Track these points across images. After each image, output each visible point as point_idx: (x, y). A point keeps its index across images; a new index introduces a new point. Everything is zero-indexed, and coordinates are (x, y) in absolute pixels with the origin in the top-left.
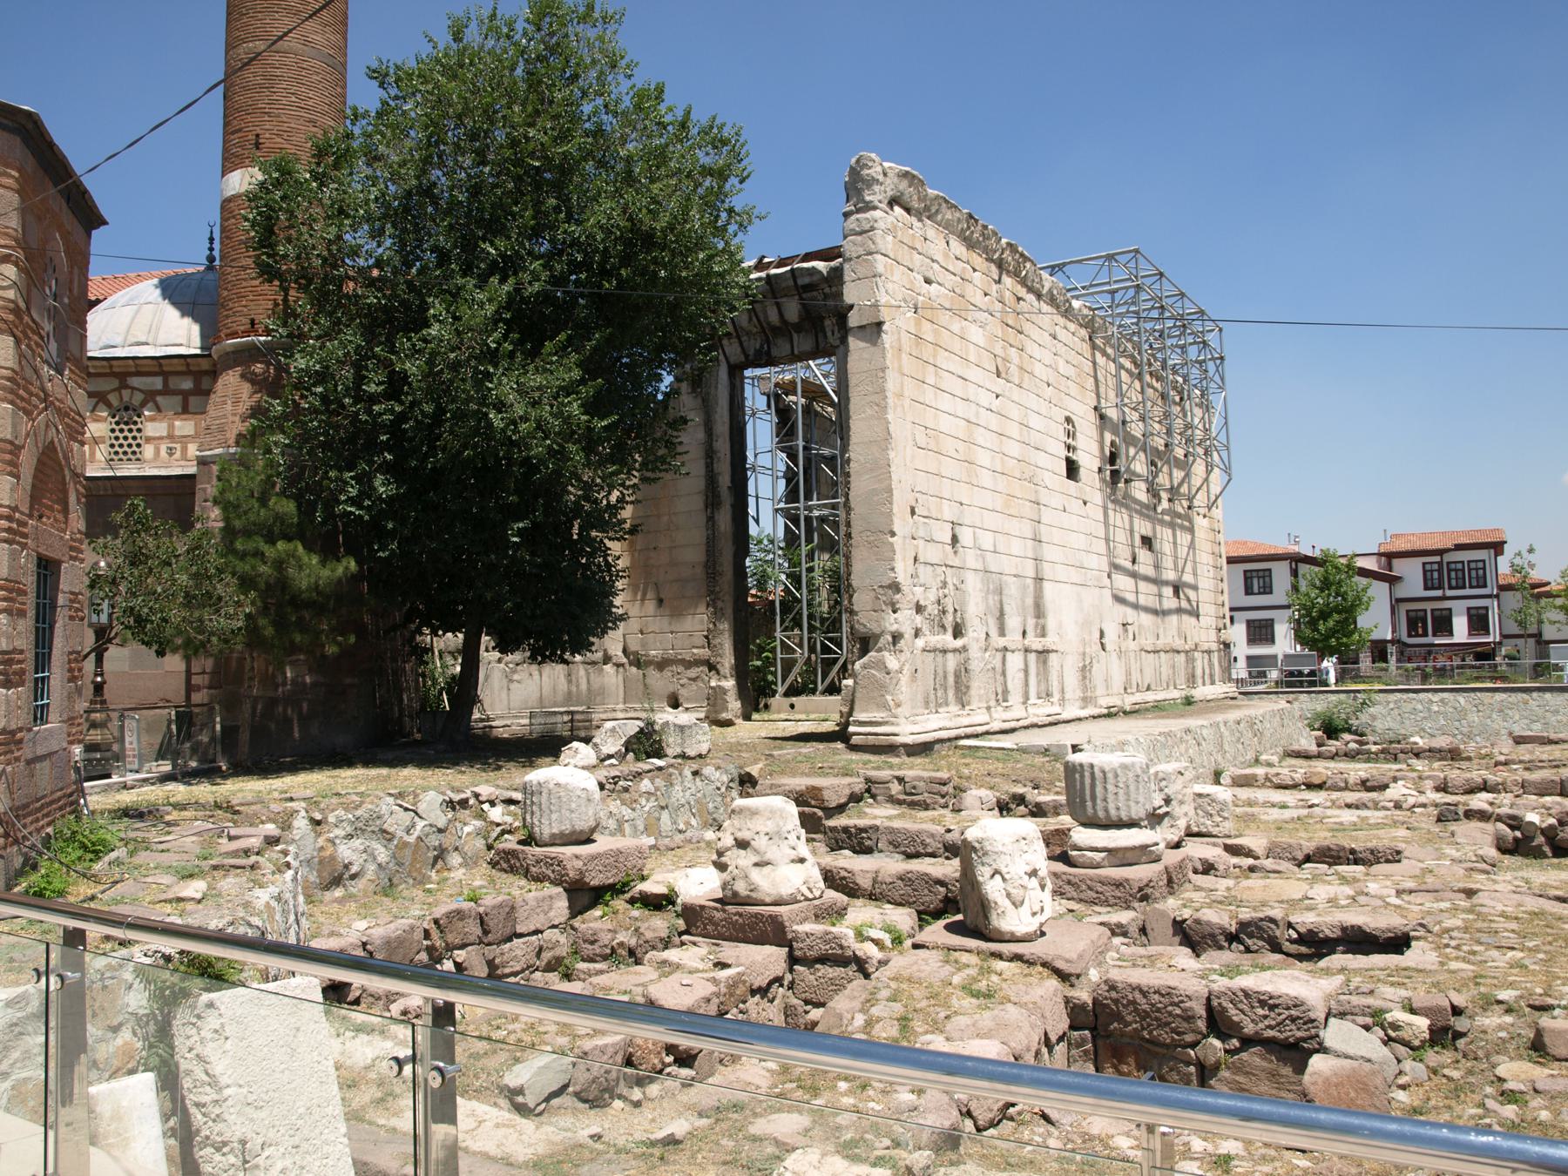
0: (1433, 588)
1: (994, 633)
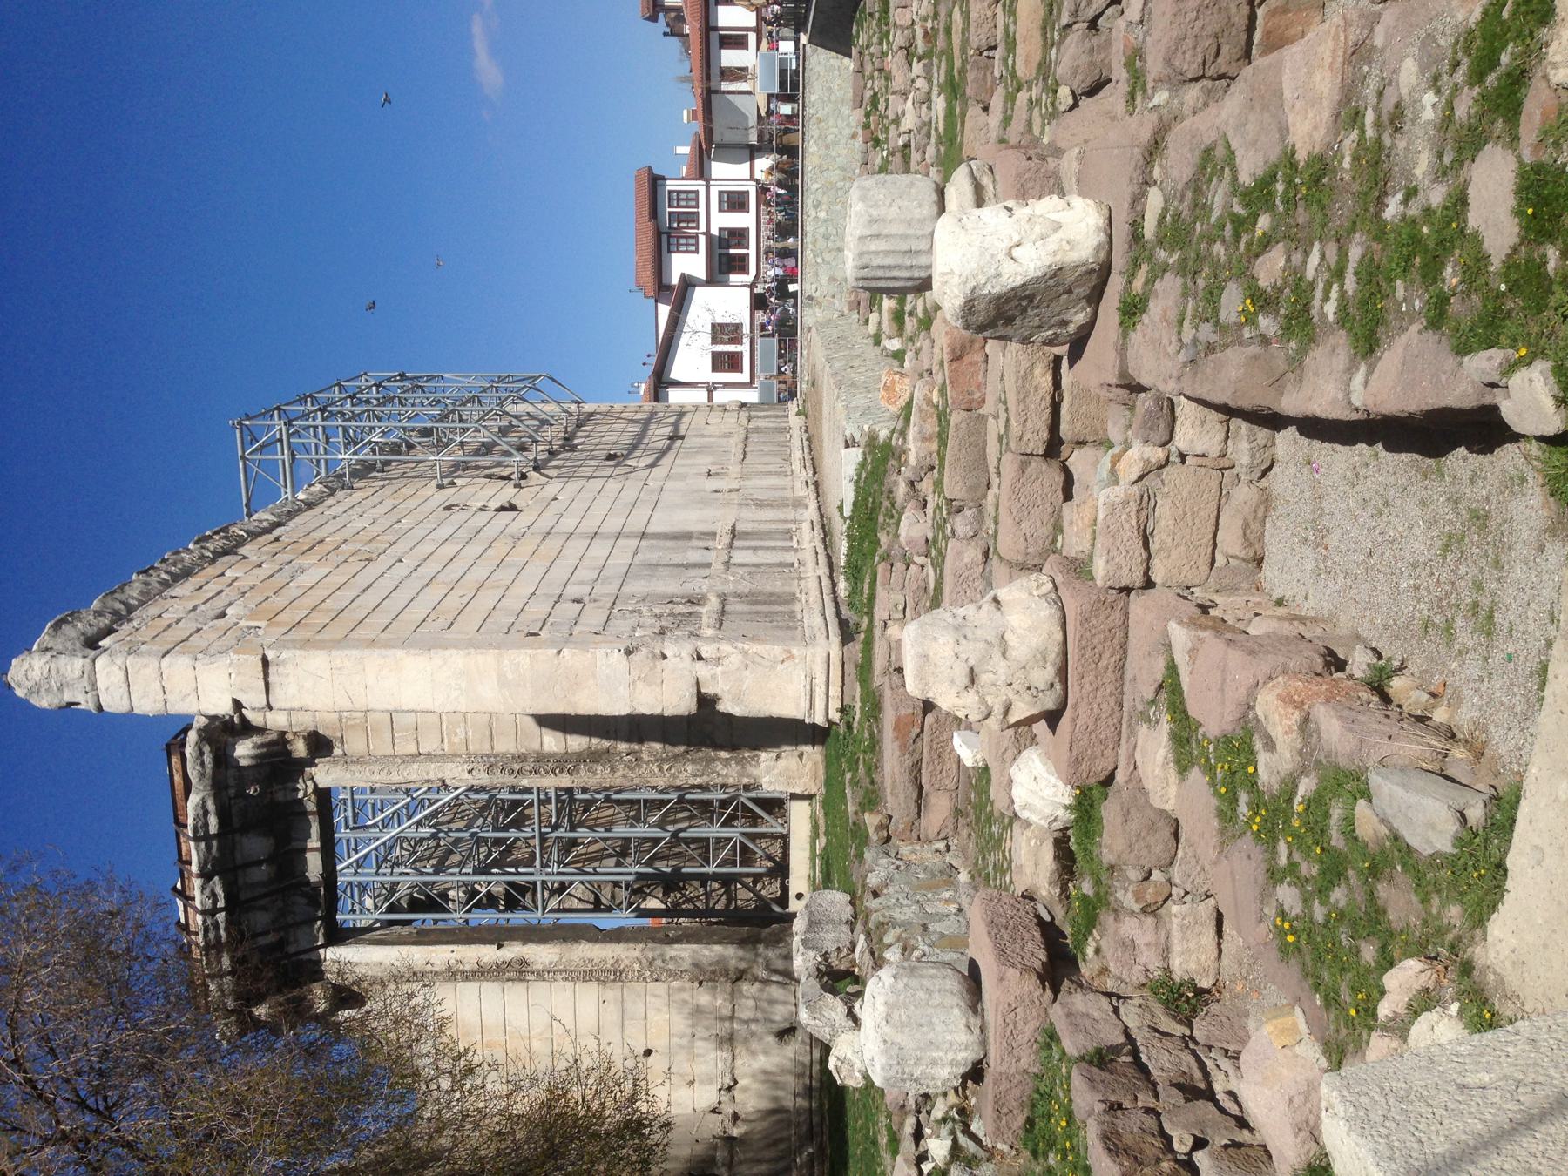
0: (697, 244)
1: (706, 572)
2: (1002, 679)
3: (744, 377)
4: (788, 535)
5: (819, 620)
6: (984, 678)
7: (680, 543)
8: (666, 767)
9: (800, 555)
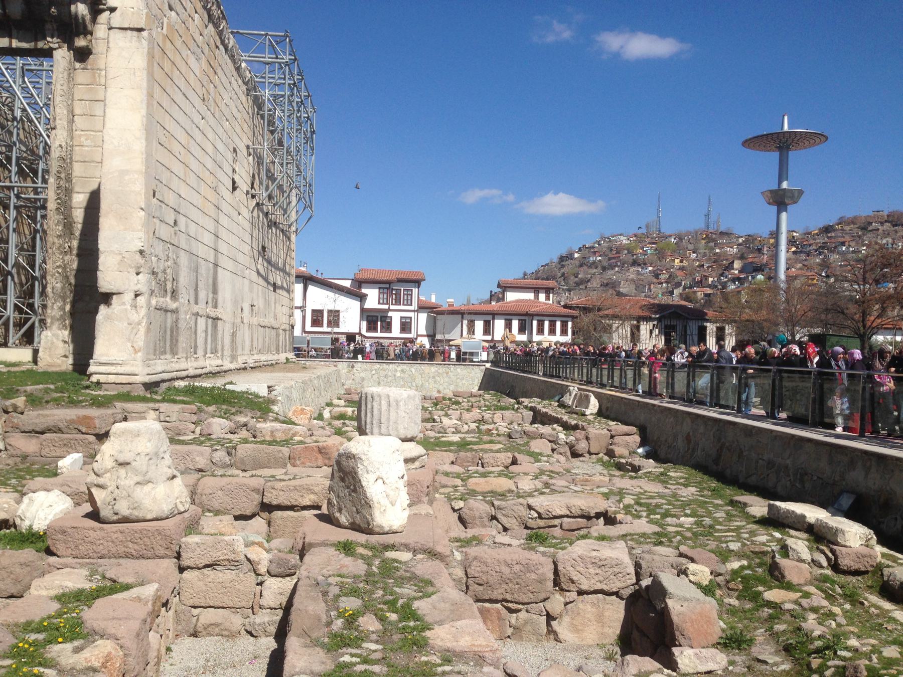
0: (383, 304)
2: (122, 483)
3: (309, 328)
4: (214, 351)
5: (160, 369)
6: (122, 471)
7: (211, 287)
8: (60, 270)
9: (202, 358)
